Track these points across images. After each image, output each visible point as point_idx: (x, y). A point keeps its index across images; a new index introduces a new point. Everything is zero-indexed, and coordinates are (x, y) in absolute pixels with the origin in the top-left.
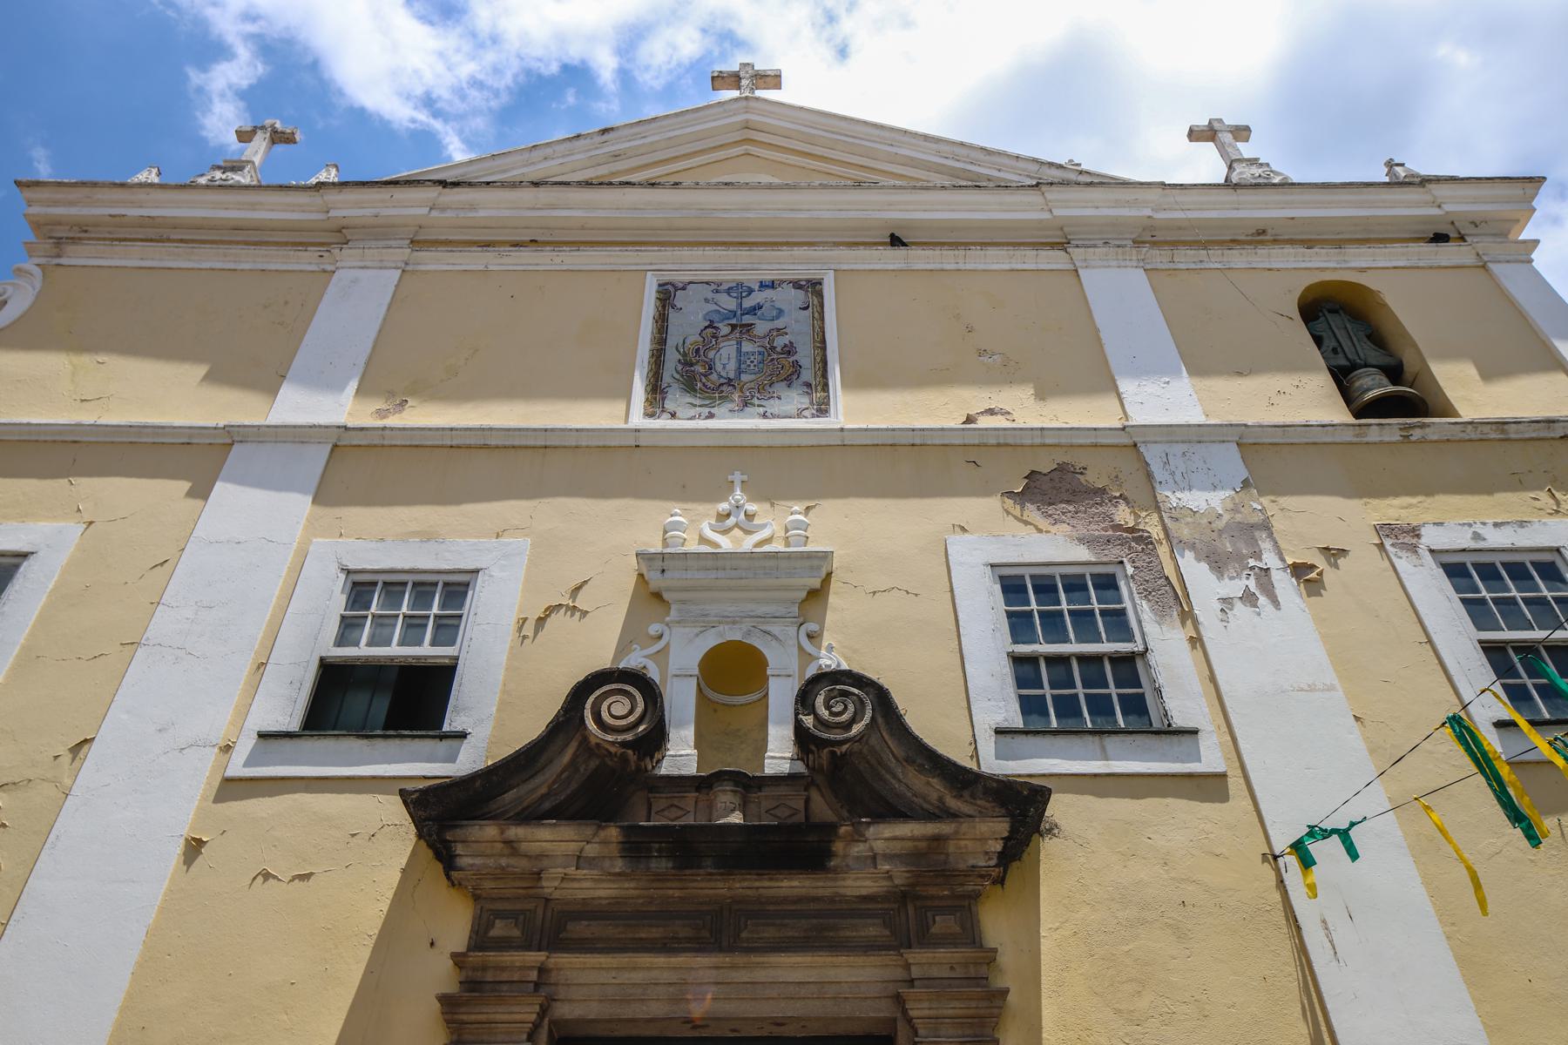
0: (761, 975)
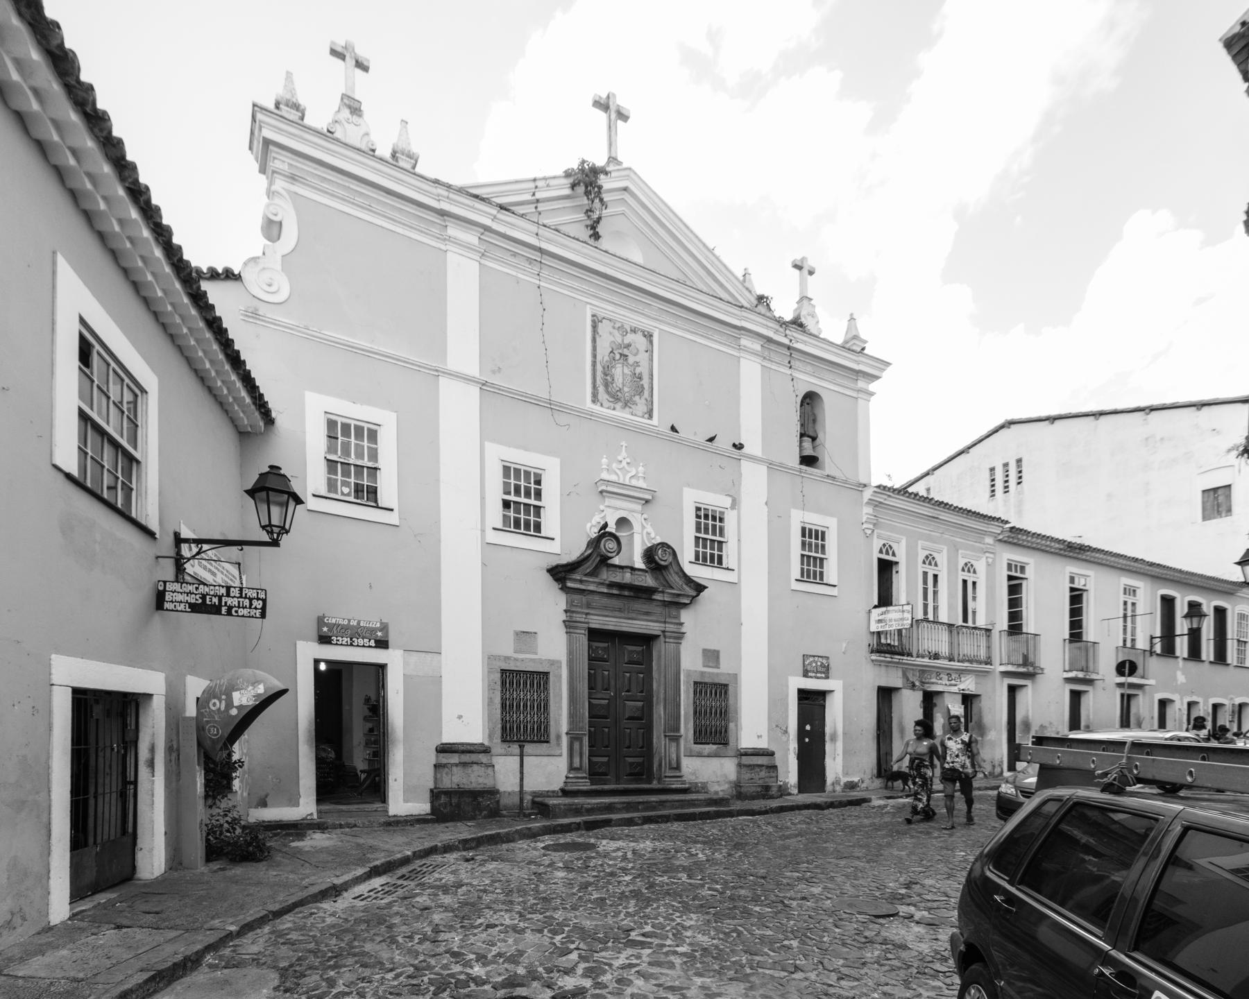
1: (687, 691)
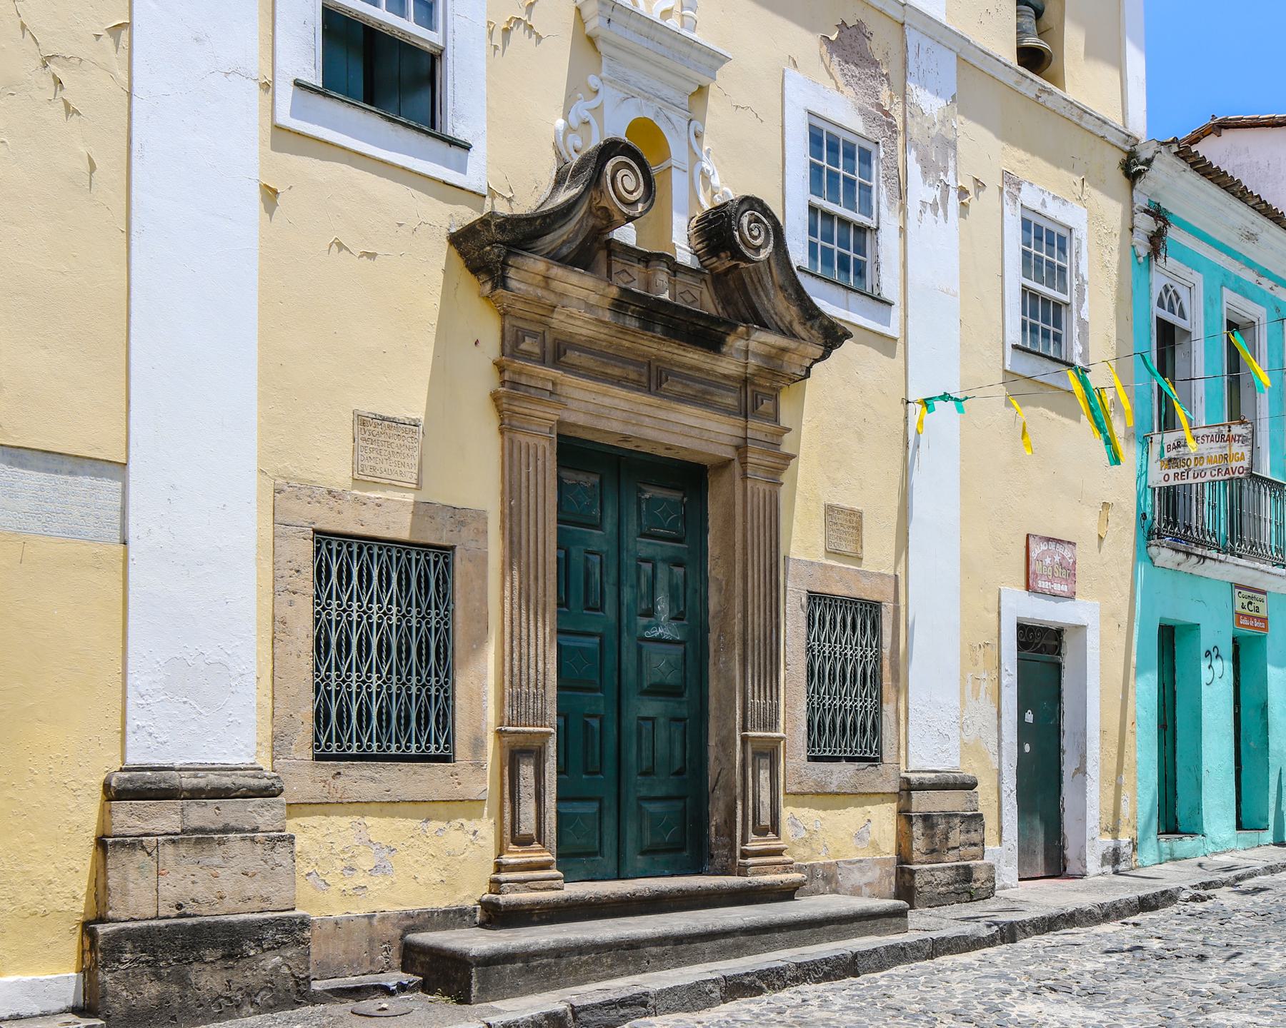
0: (673, 417)
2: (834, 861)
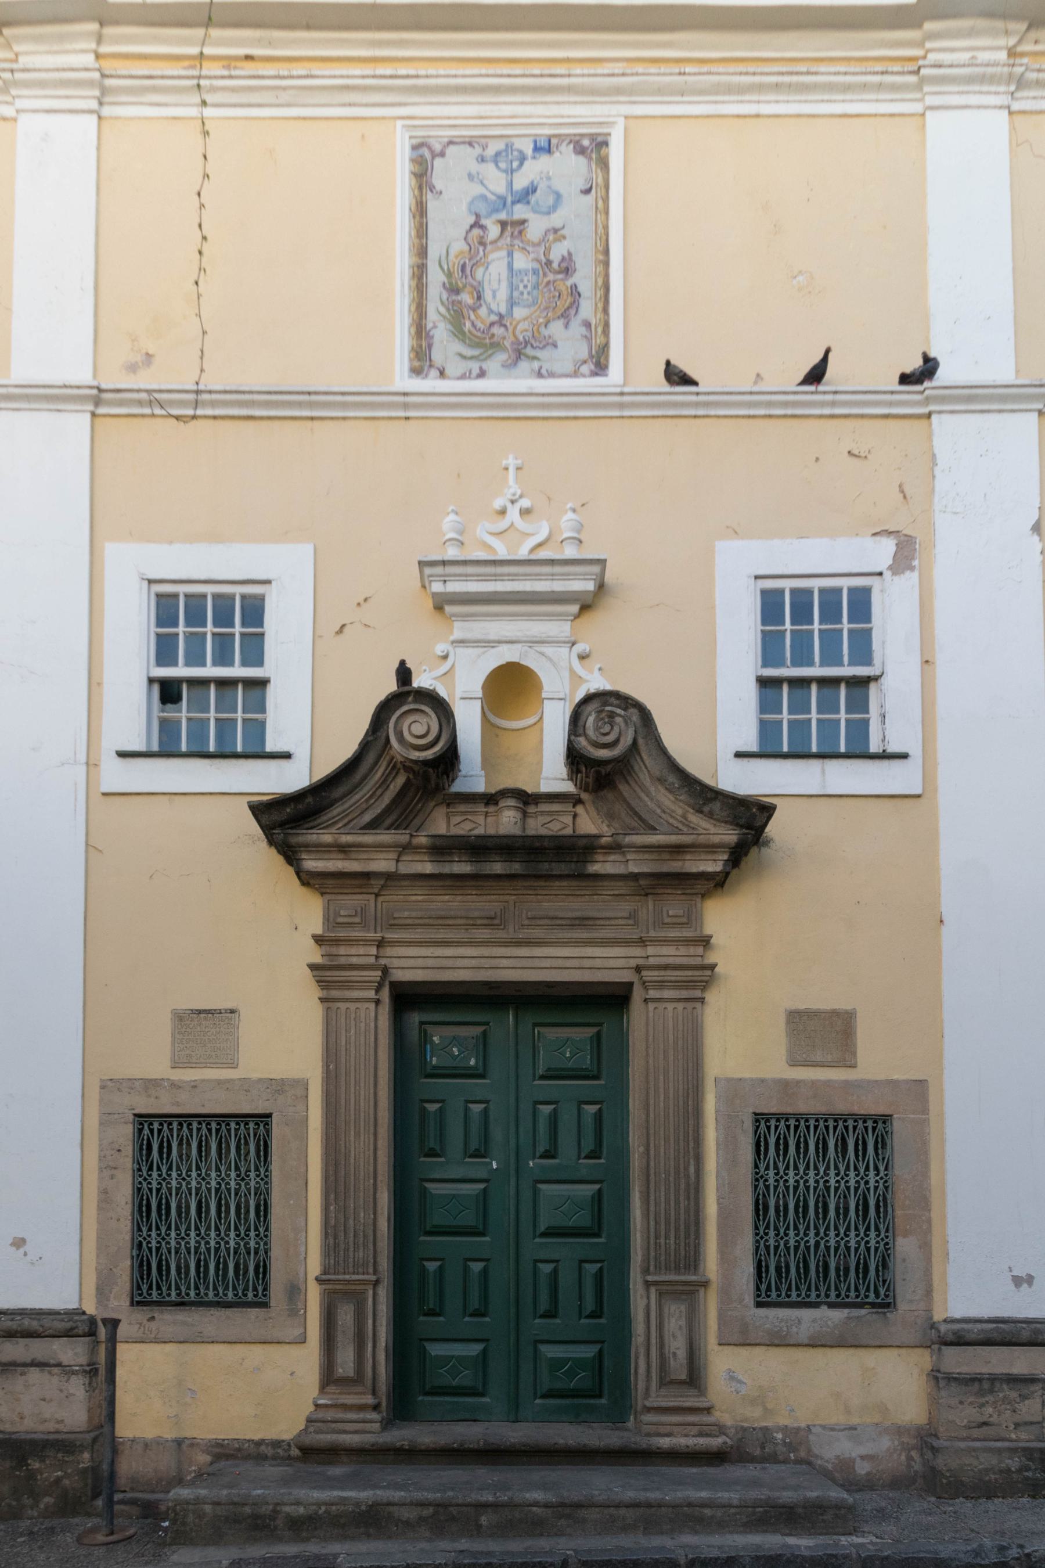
1: (728, 1143)
2: (803, 1425)
